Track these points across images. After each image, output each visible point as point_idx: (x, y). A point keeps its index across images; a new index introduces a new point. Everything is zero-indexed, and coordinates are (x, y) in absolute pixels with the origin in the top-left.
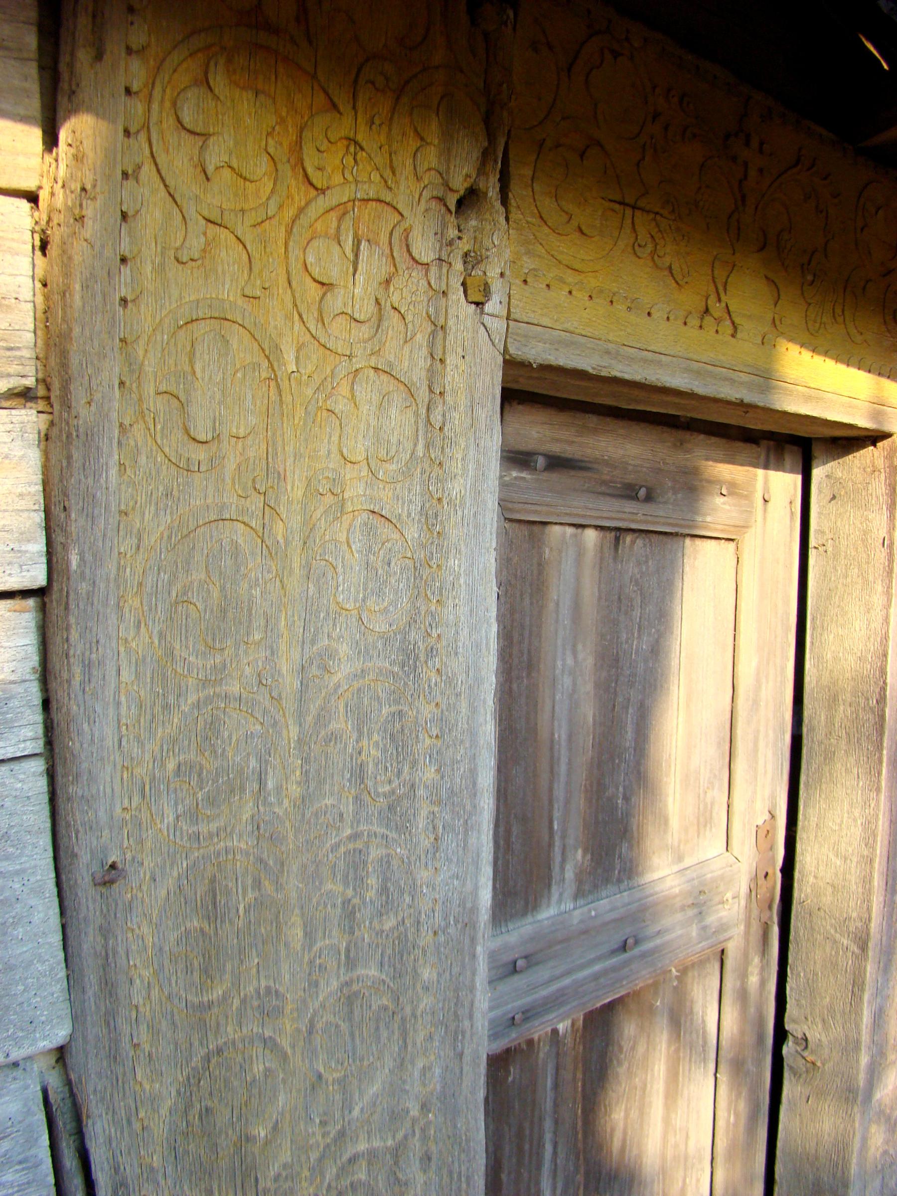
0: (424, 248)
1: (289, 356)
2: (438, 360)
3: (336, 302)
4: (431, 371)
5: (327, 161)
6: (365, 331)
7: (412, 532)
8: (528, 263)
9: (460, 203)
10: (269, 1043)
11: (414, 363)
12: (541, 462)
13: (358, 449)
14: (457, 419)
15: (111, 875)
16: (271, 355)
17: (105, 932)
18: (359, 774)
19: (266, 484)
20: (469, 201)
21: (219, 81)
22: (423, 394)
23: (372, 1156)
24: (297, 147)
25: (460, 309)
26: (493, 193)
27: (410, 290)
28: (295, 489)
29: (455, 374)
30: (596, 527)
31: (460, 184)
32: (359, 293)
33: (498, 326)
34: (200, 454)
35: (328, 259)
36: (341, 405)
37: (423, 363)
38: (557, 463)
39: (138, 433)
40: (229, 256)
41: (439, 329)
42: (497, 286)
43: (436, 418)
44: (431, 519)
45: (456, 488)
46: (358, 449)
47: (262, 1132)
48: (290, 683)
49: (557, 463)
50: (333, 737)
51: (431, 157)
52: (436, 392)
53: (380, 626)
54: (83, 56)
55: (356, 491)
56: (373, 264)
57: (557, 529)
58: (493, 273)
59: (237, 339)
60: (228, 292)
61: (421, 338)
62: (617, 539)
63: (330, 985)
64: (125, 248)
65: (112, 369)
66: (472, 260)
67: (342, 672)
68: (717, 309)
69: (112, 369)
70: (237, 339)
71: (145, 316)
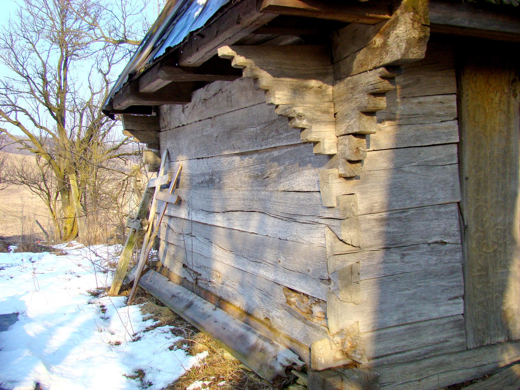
0: (506, 91)
1: (487, 110)
3: (494, 101)
6: (497, 105)
7: (506, 133)
9: (512, 82)
10: (486, 207)
11: (505, 108)
15: (467, 179)
16: (485, 110)
17: (466, 186)
18: (498, 169)
20: (514, 81)
22: (507, 112)
23: (501, 229)
25: (512, 99)
28: (489, 128)
29: (512, 109)
31: (512, 79)
32: (497, 99)
35: (492, 95)
36: (495, 116)
37: (506, 108)
41: (509, 102)
45: (512, 126)
47: (485, 220)
48: (488, 155)
50: (494, 163)
53: (501, 147)
55: (497, 128)
56: (499, 95)
61: (506, 104)
63: (494, 200)
64: (467, 99)
66: (514, 91)
67: (496, 154)
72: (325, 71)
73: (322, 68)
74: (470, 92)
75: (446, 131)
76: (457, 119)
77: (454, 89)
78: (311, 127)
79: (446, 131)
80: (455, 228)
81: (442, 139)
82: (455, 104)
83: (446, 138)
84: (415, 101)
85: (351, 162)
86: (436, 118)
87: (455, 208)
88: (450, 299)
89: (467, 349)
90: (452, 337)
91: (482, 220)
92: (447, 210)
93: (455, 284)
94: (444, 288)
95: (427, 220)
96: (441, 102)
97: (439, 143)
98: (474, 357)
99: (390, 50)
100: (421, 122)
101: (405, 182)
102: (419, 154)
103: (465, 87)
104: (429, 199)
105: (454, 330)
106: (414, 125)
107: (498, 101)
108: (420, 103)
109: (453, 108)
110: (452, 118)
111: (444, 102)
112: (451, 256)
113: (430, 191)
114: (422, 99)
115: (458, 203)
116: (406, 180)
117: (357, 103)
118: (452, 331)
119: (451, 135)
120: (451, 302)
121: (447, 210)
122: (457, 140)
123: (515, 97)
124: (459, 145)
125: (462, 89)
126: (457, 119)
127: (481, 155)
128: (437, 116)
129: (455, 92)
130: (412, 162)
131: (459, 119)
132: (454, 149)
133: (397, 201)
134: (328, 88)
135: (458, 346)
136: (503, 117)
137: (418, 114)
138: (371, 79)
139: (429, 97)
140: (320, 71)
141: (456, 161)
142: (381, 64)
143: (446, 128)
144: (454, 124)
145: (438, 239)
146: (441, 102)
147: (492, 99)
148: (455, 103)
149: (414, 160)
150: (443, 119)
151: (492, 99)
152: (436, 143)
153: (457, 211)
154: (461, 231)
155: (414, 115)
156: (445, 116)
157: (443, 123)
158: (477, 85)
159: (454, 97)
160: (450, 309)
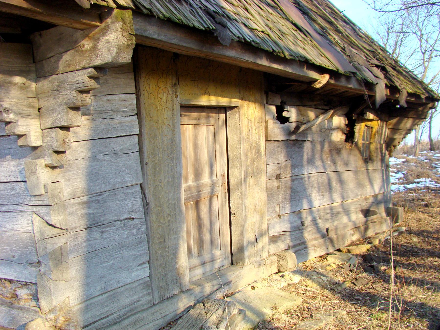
0: (170, 92)
2: (173, 105)
3: (162, 100)
5: (160, 84)
6: (165, 103)
7: (171, 126)
8: (182, 91)
10: (161, 186)
11: (170, 106)
13: (165, 117)
14: (175, 112)
15: (147, 164)
16: (157, 107)
18: (168, 155)
19: (157, 122)
21: (150, 78)
23: (172, 204)
24: (157, 83)
26: (177, 83)
27: (169, 97)
28: (160, 122)
29: (175, 107)
31: (174, 83)
32: (164, 99)
33: (179, 100)
34: (151, 119)
35: (161, 95)
36: (164, 112)
37: (171, 106)
39: (147, 118)
40: (152, 97)
41: (173, 102)
42: (179, 95)
44: (173, 124)
45: (176, 121)
46: (165, 117)
48: (161, 144)
50: (165, 150)
51: (170, 81)
52: (173, 109)
53: (169, 137)
54: (139, 79)
56: (166, 95)
58: (178, 94)
59: (154, 106)
60: (153, 101)
61: (171, 103)
63: (166, 180)
66: (176, 92)
67: (166, 142)
68: (207, 92)
71: (146, 105)
72: (28, 69)
73: (25, 65)
74: (145, 93)
75: (130, 124)
76: (137, 114)
77: (133, 90)
78: (18, 120)
80: (139, 205)
81: (127, 131)
82: (134, 102)
84: (105, 98)
85: (58, 152)
86: (122, 113)
87: (138, 188)
88: (139, 265)
89: (154, 304)
90: (142, 297)
91: (159, 197)
92: (133, 190)
93: (142, 252)
94: (135, 256)
95: (119, 201)
97: (125, 134)
98: (160, 310)
99: (100, 53)
100: (110, 117)
101: (100, 168)
102: (110, 144)
103: (142, 88)
104: (119, 183)
105: (143, 290)
106: (105, 120)
107: (165, 101)
108: (109, 100)
109: (134, 105)
110: (133, 114)
111: (127, 100)
112: (138, 229)
113: (120, 176)
114: (110, 97)
115: (141, 184)
116: (101, 167)
117: (64, 99)
118: (142, 291)
119: (133, 128)
120: (140, 267)
121: (133, 190)
122: (138, 132)
124: (140, 136)
125: (140, 89)
126: (137, 114)
127: (156, 144)
128: (123, 112)
129: (135, 92)
130: (104, 152)
131: (138, 114)
132: (136, 139)
133: (94, 186)
134: (32, 84)
135: (148, 303)
136: (169, 113)
137: (107, 110)
138: (79, 78)
139: (115, 96)
140: (24, 69)
141: (137, 149)
142: (91, 65)
143: (129, 122)
145: (127, 216)
147: (161, 99)
148: (135, 101)
149: (106, 150)
151: (161, 99)
152: (122, 135)
153: (140, 190)
154: (144, 207)
155: (104, 110)
156: (128, 112)
157: (127, 118)
158: (151, 87)
159: (134, 96)
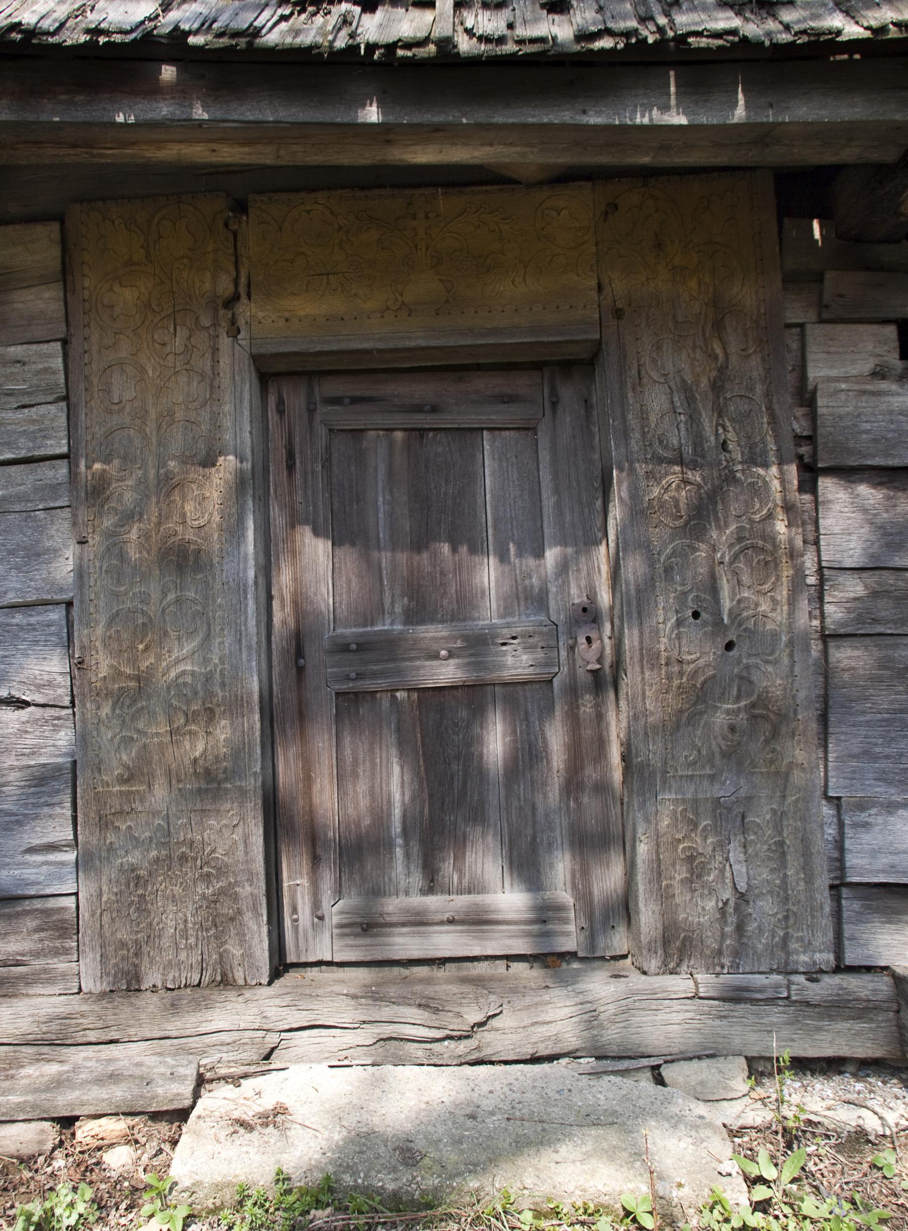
0: (206, 321)
2: (215, 361)
4: (213, 367)
12: (347, 401)
25: (225, 342)
30: (405, 430)
38: (355, 400)
41: (215, 350)
43: (216, 384)
49: (355, 400)
56: (182, 333)
57: (372, 432)
62: (422, 436)
64: (86, 348)
65: (82, 386)
69: (82, 386)
70: (129, 369)
79: (32, 428)
81: (18, 448)
83: (31, 445)
90: (37, 954)
92: (33, 620)
94: (13, 818)
96: (19, 362)
105: (43, 934)
109: (54, 373)
111: (26, 360)
112: (40, 737)
115: (69, 604)
118: (36, 936)
121: (33, 620)
123: (235, 337)
128: (7, 395)
144: (57, 414)
146: (19, 362)
150: (26, 400)
156: (28, 393)
157: (26, 411)
160: (33, 877)
